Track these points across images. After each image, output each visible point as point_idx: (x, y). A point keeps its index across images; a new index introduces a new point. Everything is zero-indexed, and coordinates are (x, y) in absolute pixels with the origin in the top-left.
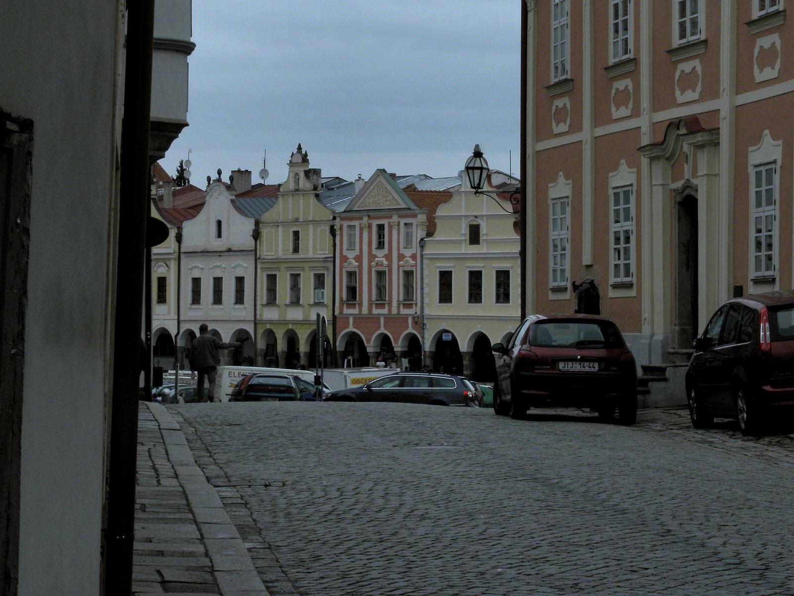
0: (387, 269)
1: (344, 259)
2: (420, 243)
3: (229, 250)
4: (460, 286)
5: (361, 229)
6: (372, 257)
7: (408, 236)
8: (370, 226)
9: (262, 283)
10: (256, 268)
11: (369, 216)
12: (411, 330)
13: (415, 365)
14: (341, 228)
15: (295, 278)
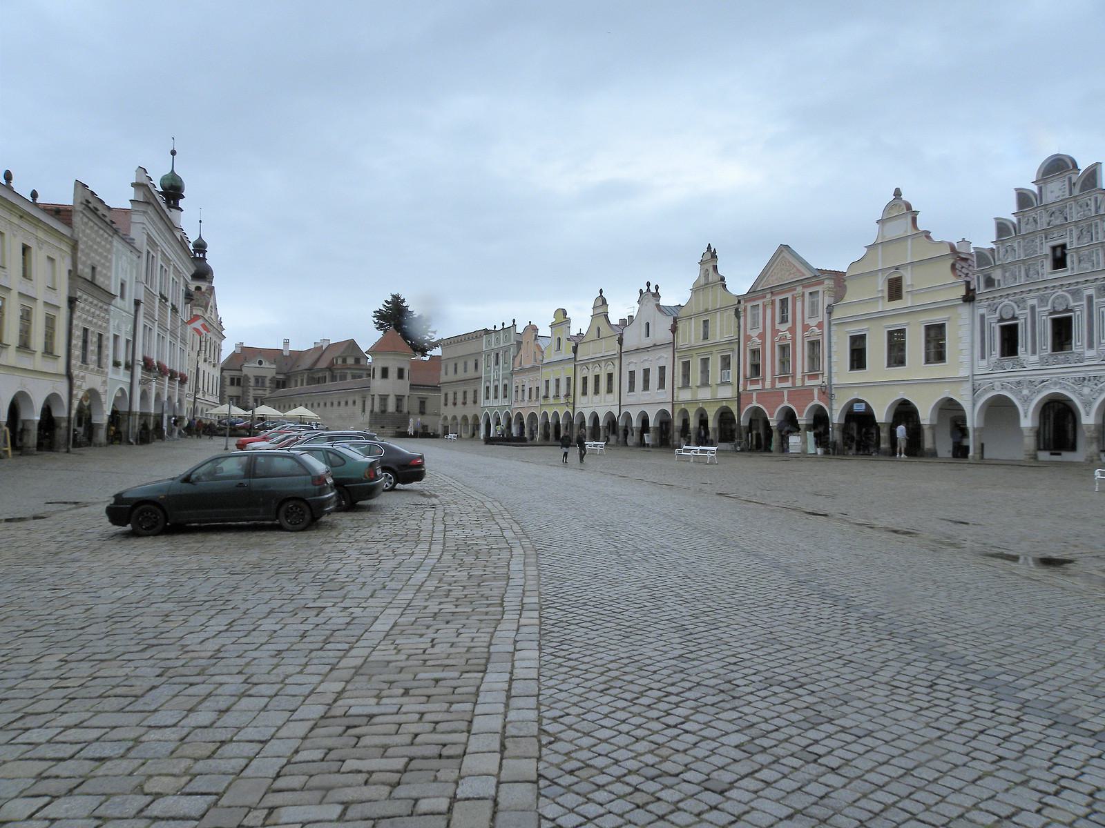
0: (790, 342)
1: (748, 338)
2: (827, 308)
3: (655, 345)
4: (877, 350)
5: (764, 307)
6: (775, 332)
7: (814, 307)
8: (773, 303)
9: (678, 369)
10: (674, 357)
11: (772, 293)
12: (816, 402)
13: (822, 440)
14: (745, 310)
15: (705, 362)
